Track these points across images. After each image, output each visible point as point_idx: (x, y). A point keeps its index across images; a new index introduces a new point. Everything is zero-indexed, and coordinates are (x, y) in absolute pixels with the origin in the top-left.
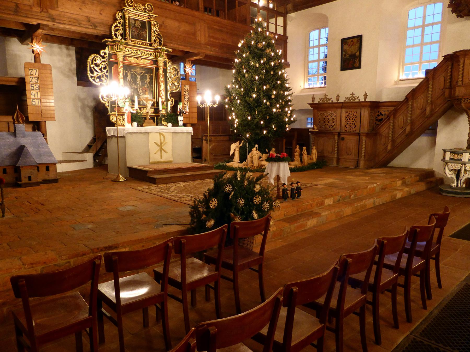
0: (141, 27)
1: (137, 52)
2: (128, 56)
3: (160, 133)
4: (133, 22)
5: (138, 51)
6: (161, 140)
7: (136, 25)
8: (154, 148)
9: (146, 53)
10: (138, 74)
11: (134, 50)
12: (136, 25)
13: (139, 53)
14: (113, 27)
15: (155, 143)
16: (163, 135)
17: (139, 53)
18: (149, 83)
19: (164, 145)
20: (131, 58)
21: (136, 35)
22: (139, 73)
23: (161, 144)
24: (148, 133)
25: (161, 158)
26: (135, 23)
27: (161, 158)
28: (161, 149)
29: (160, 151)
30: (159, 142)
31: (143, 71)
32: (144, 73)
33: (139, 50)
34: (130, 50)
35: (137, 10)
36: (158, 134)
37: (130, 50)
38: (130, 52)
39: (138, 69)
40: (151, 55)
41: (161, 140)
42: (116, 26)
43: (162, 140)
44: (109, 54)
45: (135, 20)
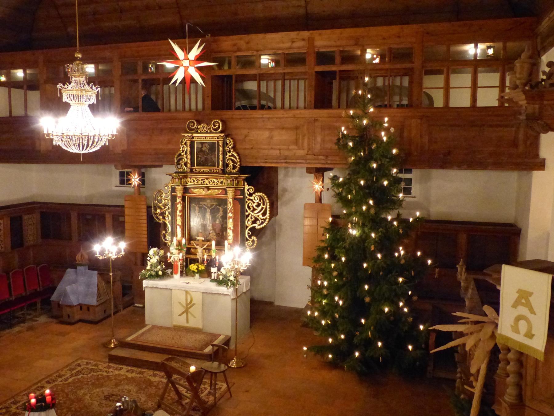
0: (209, 150)
1: (204, 182)
2: (193, 188)
3: (187, 292)
4: (200, 146)
5: (206, 180)
6: (186, 300)
7: (203, 149)
8: (178, 309)
9: (216, 181)
10: (208, 207)
11: (201, 179)
12: (203, 149)
13: (207, 182)
14: (176, 156)
15: (179, 303)
16: (190, 294)
17: (207, 182)
18: (222, 217)
19: (191, 307)
20: (196, 190)
21: (202, 161)
22: (209, 206)
23: (187, 304)
24: (171, 289)
25: (187, 322)
26: (202, 147)
27: (187, 322)
28: (186, 311)
29: (185, 315)
30: (185, 302)
31: (215, 204)
32: (217, 205)
33: (207, 179)
34: (195, 179)
35: (201, 133)
36: (184, 293)
37: (195, 179)
38: (196, 182)
39: (208, 201)
40: (222, 182)
41: (186, 300)
42: (180, 155)
43: (189, 301)
44: (172, 187)
45: (202, 143)
